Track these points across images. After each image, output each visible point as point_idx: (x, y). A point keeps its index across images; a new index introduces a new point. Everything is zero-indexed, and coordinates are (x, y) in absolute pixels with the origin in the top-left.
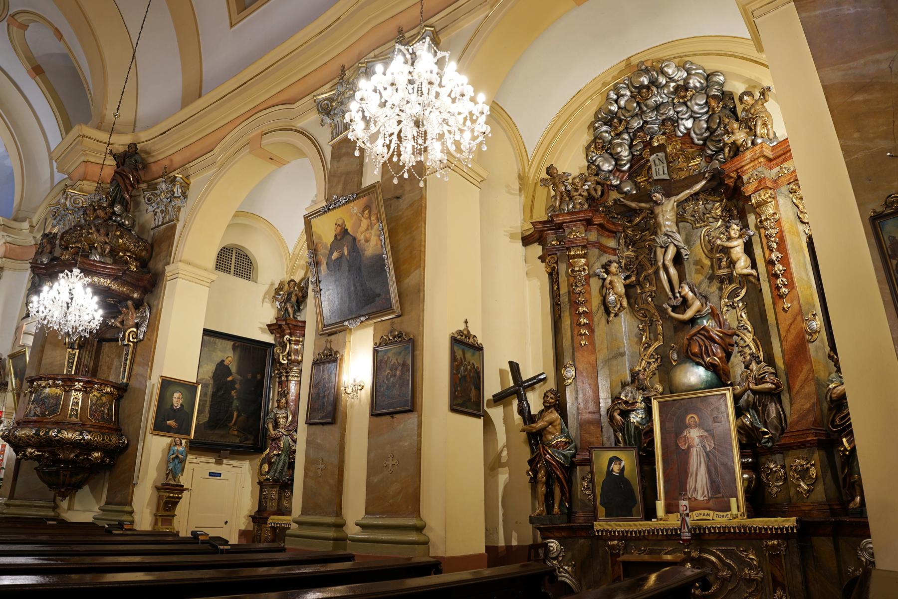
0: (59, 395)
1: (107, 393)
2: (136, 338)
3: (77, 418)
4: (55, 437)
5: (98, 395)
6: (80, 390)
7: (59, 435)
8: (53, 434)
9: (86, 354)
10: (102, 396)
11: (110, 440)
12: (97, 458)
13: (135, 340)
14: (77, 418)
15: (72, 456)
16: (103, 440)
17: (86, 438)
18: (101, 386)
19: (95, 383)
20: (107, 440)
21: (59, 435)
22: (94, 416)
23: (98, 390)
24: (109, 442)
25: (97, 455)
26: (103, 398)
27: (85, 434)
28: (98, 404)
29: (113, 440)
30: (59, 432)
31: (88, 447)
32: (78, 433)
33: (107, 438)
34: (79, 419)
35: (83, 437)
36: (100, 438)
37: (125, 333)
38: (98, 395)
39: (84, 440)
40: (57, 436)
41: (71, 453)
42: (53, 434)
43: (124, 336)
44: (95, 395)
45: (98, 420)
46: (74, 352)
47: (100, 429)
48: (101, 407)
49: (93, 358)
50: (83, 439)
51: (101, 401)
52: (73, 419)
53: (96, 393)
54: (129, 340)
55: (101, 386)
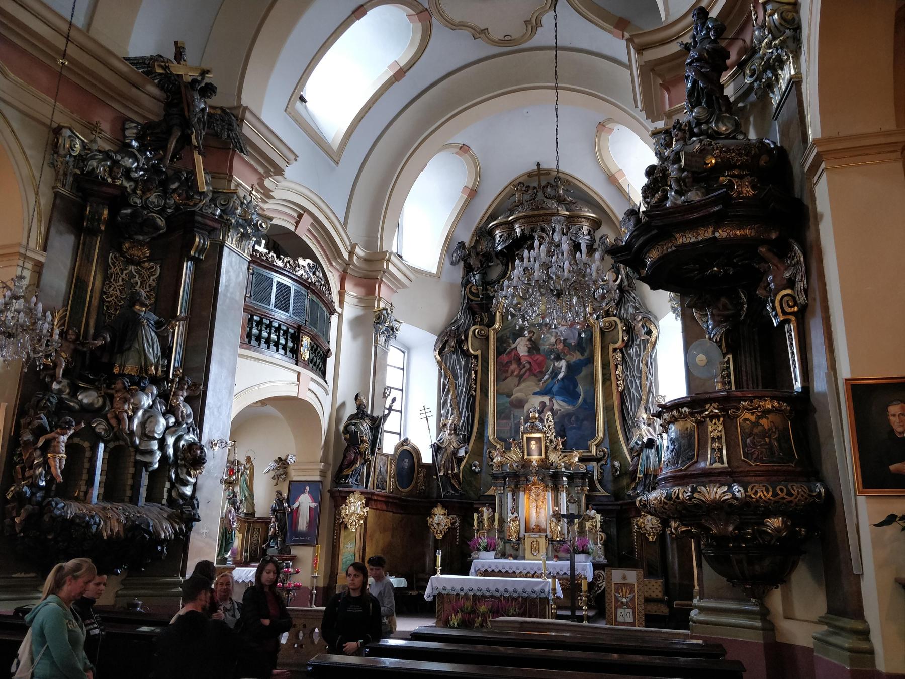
0: (691, 430)
1: (768, 412)
2: (795, 304)
3: (723, 463)
4: (690, 500)
5: (753, 418)
6: (717, 417)
7: (696, 495)
8: (685, 495)
9: (745, 357)
10: (759, 418)
11: (789, 494)
12: (777, 530)
13: (796, 309)
14: (723, 463)
15: (731, 528)
16: (775, 495)
17: (738, 495)
18: (751, 402)
19: (740, 400)
20: (781, 495)
21: (696, 495)
22: (752, 454)
23: (749, 410)
24: (789, 499)
25: (775, 522)
26: (764, 422)
27: (736, 488)
28: (756, 434)
29: (795, 493)
30: (694, 490)
31: (761, 511)
32: (726, 489)
33: (781, 490)
34: (726, 465)
35: (733, 494)
36: (768, 491)
37: (773, 302)
38: (753, 418)
39: (736, 499)
40: (691, 498)
41: (727, 525)
42: (685, 495)
43: (774, 309)
44: (746, 420)
45: (761, 461)
46: (726, 359)
47: (770, 477)
48: (764, 437)
49: (758, 360)
50: (734, 497)
51: (760, 428)
52: (717, 465)
53: (748, 416)
54: (784, 313)
55: (751, 402)
